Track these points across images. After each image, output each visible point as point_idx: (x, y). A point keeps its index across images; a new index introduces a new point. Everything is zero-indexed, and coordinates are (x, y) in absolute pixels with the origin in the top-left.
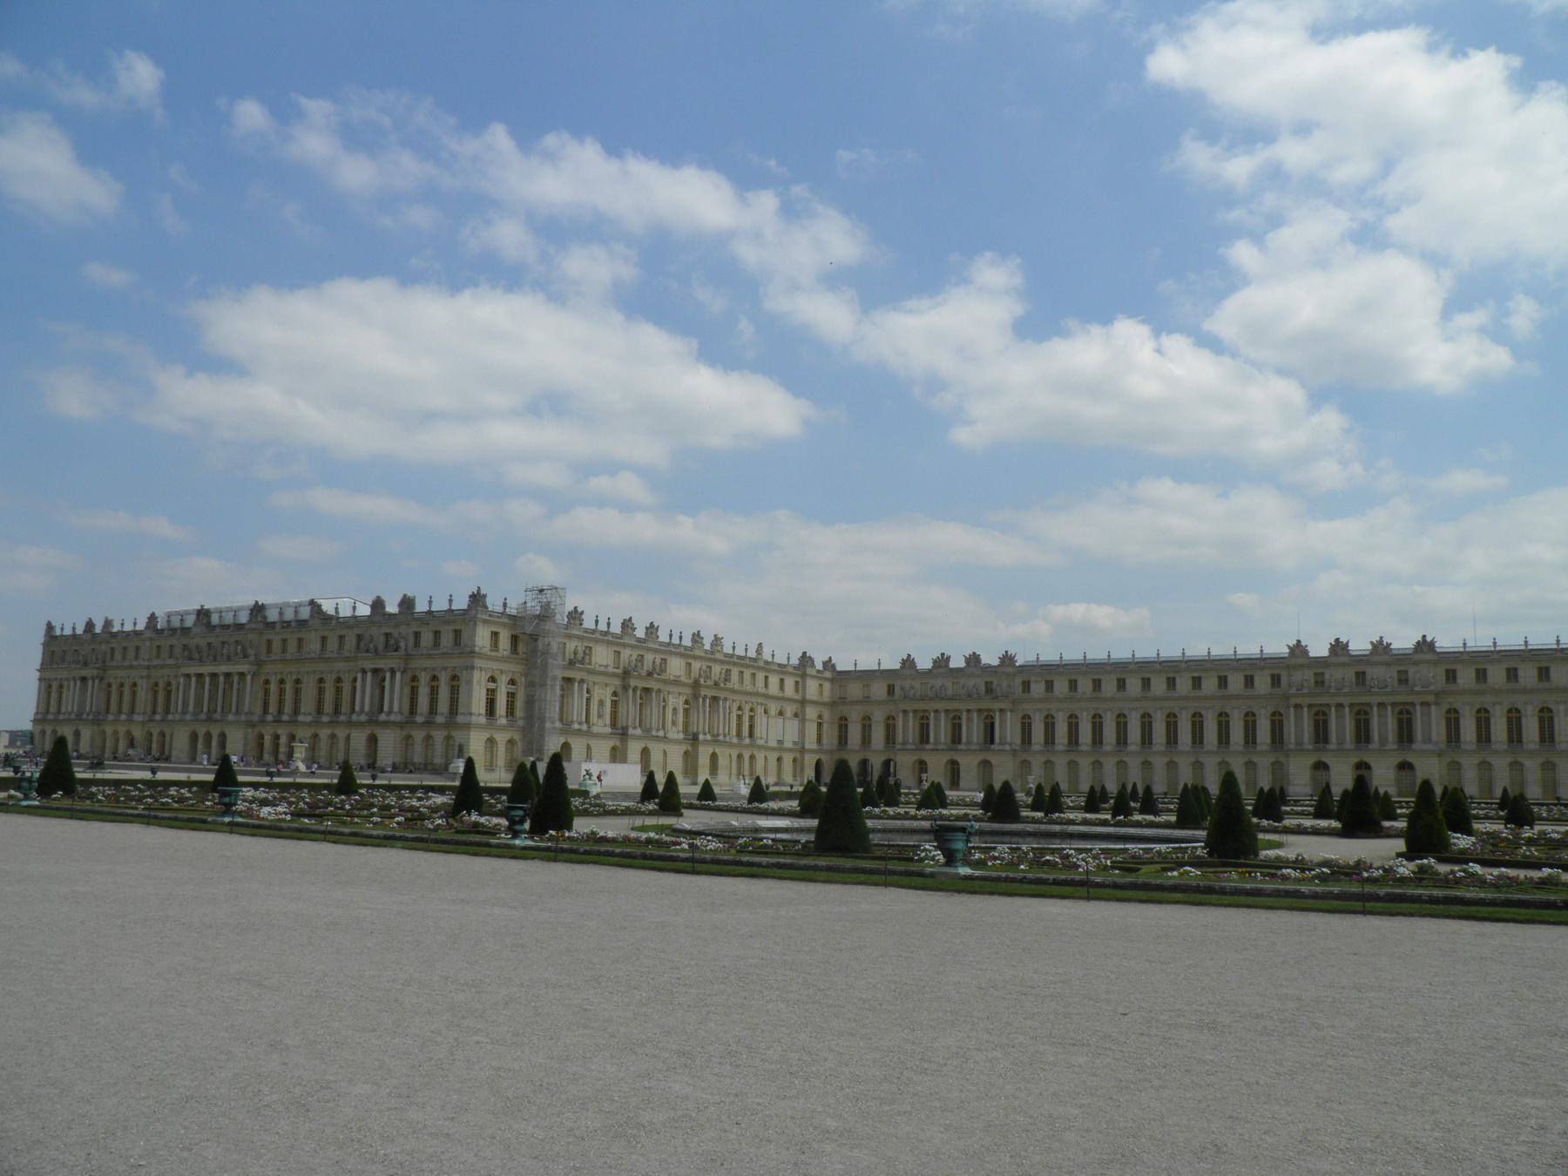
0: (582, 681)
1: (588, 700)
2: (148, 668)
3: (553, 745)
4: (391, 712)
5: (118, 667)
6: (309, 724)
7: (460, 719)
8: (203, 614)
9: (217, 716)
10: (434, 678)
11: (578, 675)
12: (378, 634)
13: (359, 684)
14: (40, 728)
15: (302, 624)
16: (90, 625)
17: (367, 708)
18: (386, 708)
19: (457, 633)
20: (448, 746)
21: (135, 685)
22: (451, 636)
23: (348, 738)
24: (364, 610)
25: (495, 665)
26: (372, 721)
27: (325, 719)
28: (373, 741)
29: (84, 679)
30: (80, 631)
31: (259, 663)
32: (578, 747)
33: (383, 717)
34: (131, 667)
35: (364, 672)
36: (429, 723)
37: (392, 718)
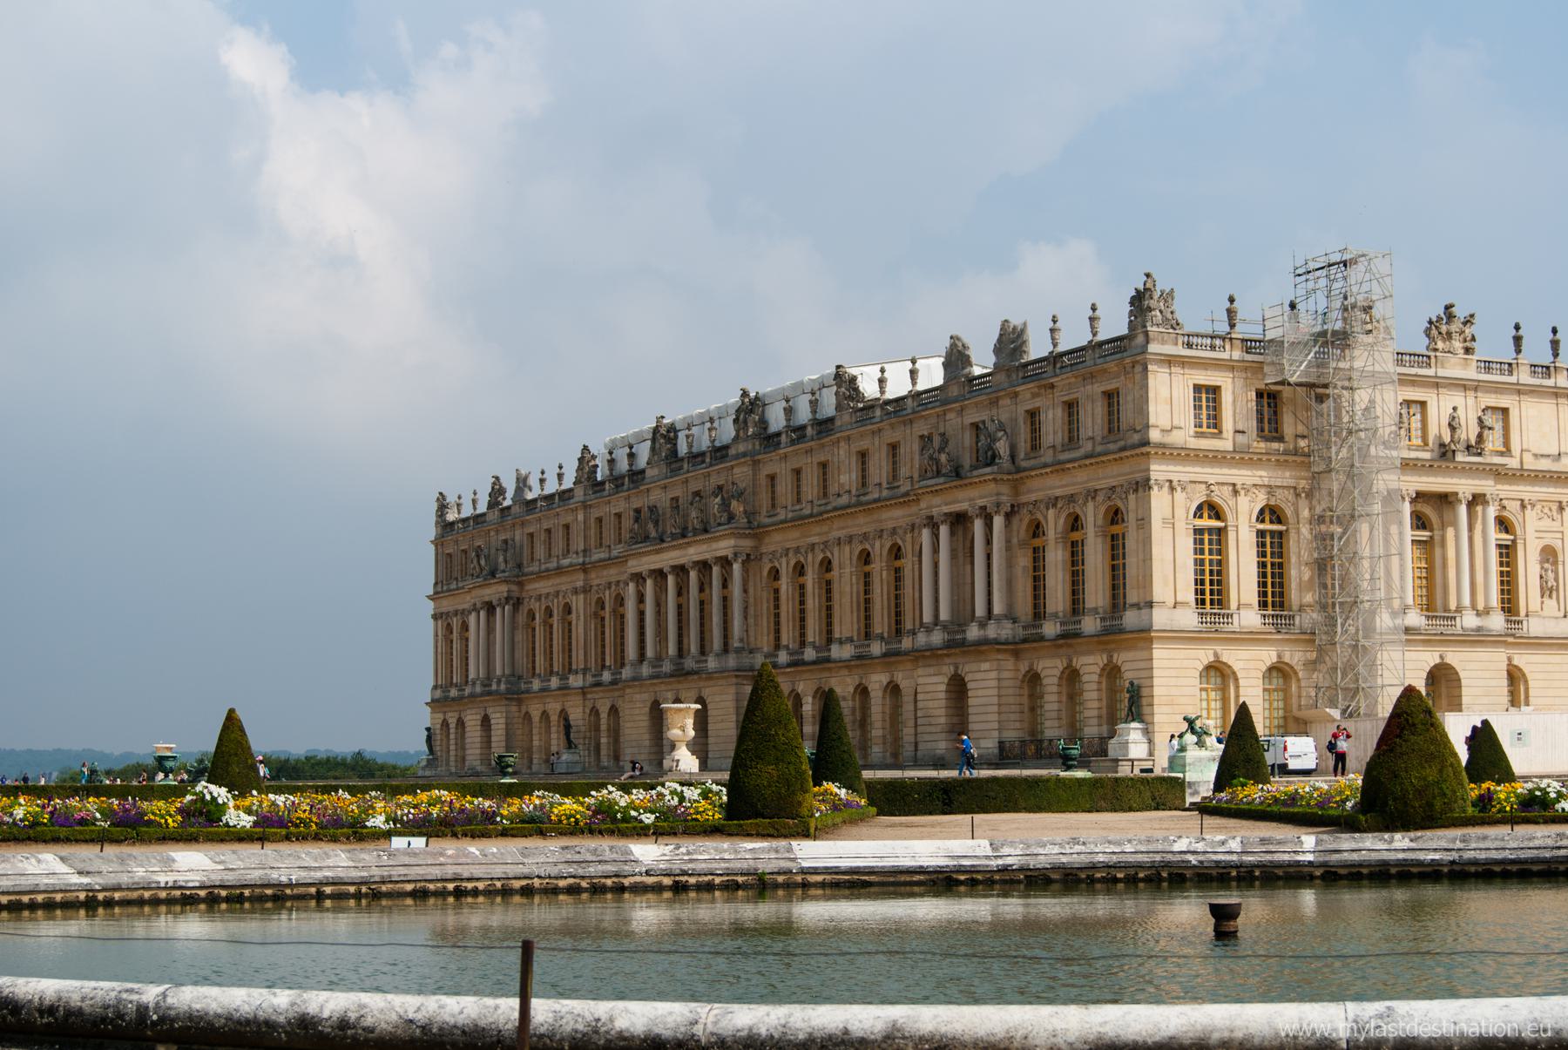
0: (1477, 500)
1: (1507, 553)
2: (584, 568)
3: (1400, 669)
5: (541, 575)
6: (846, 665)
7: (1130, 618)
8: (664, 436)
9: (689, 664)
11: (1464, 486)
12: (957, 424)
14: (441, 716)
15: (824, 426)
16: (497, 491)
17: (944, 615)
20: (1113, 691)
21: (568, 609)
22: (1100, 408)
24: (932, 375)
25: (1214, 474)
26: (956, 645)
27: (876, 648)
28: (958, 689)
29: (490, 608)
30: (482, 508)
31: (755, 530)
32: (1480, 673)
34: (560, 571)
35: (932, 524)
36: (1070, 637)
37: (992, 631)
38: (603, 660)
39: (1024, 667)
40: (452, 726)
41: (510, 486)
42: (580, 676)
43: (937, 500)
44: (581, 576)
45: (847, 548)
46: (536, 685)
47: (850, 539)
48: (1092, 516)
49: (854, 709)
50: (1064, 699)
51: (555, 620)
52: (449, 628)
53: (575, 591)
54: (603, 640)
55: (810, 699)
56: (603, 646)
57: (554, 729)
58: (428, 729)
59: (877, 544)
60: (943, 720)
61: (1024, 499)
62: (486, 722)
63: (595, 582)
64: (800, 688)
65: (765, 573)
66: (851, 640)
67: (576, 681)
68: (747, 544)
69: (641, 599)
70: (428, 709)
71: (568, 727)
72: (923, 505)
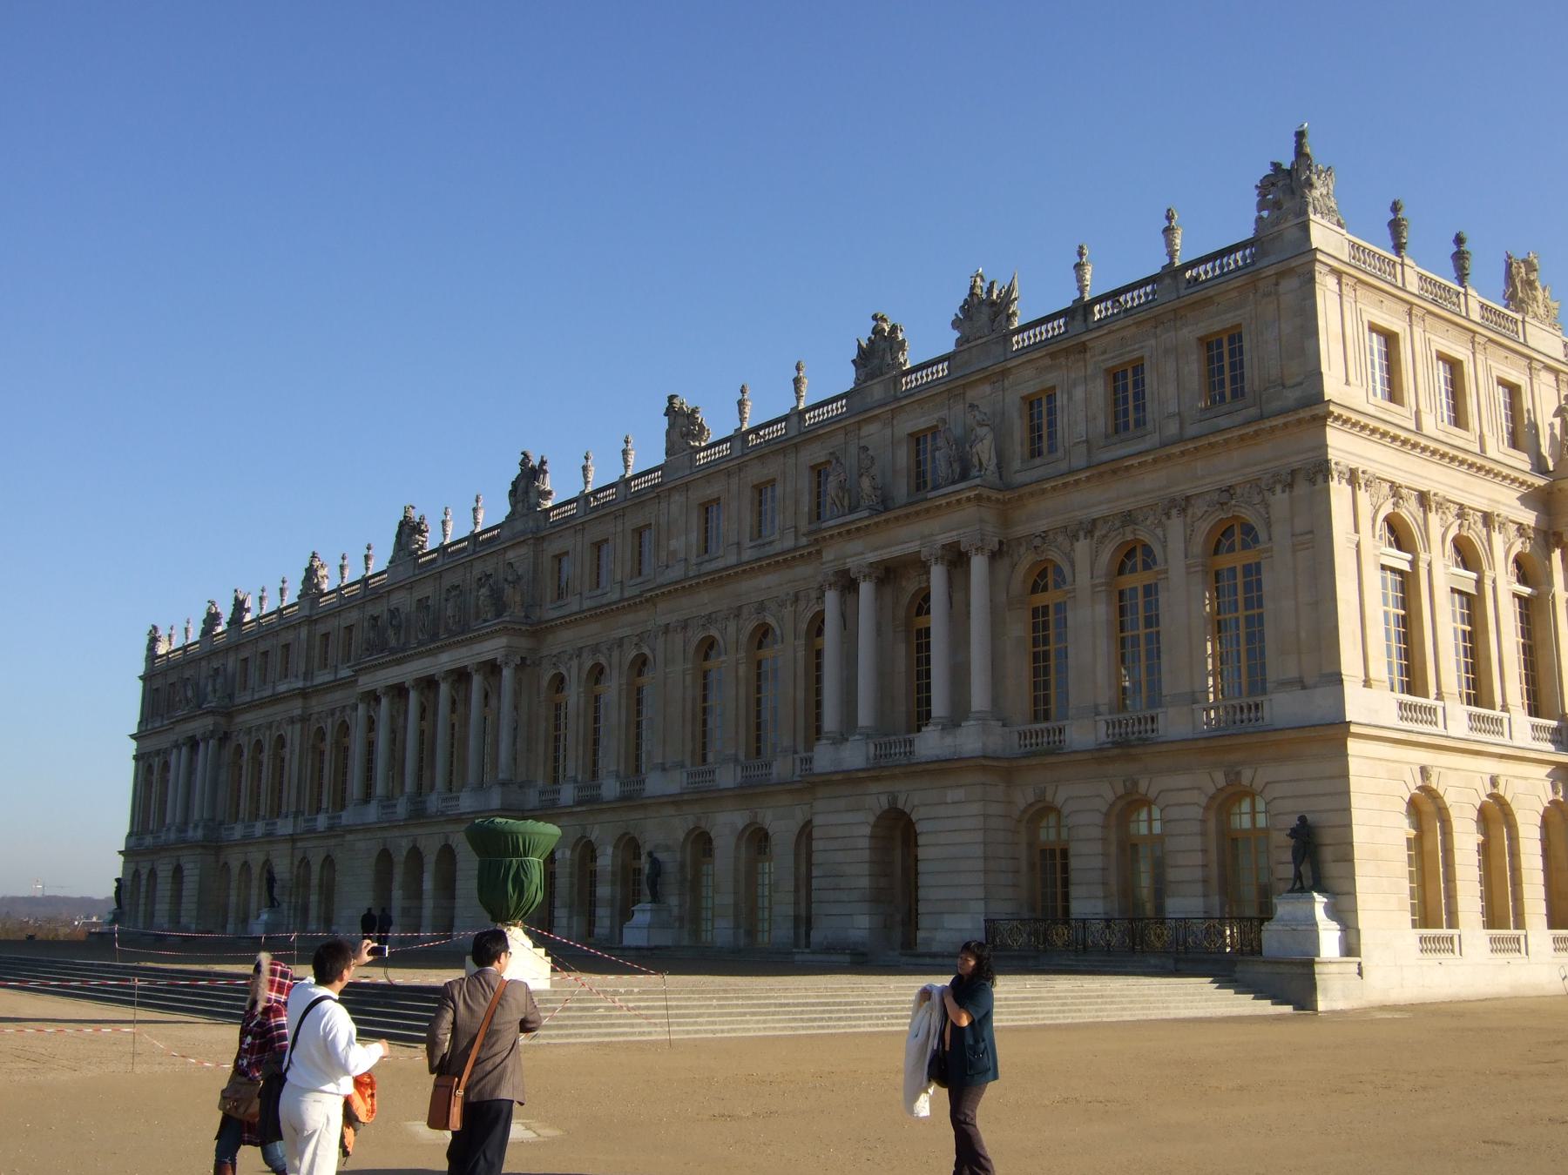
2: (304, 694)
4: (959, 715)
6: (676, 801)
10: (1133, 556)
12: (886, 442)
13: (830, 640)
14: (133, 866)
17: (865, 717)
18: (939, 706)
19: (1223, 357)
23: (806, 833)
28: (898, 832)
29: (193, 743)
30: (195, 635)
33: (930, 743)
34: (276, 699)
35: (847, 584)
36: (1129, 743)
38: (320, 801)
39: (1024, 797)
40: (144, 877)
41: (226, 613)
42: (291, 819)
43: (856, 545)
44: (299, 703)
45: (678, 638)
46: (238, 832)
47: (685, 625)
48: (1177, 547)
49: (682, 865)
50: (1113, 849)
51: (266, 757)
52: (150, 769)
53: (292, 721)
54: (321, 777)
55: (610, 850)
56: (320, 785)
57: (255, 883)
58: (118, 880)
59: (732, 628)
60: (865, 882)
61: (1021, 530)
62: (178, 871)
63: (316, 709)
64: (595, 834)
65: (545, 682)
66: (683, 766)
67: (285, 827)
68: (524, 643)
69: (371, 724)
70: (121, 858)
71: (271, 881)
72: (828, 555)
